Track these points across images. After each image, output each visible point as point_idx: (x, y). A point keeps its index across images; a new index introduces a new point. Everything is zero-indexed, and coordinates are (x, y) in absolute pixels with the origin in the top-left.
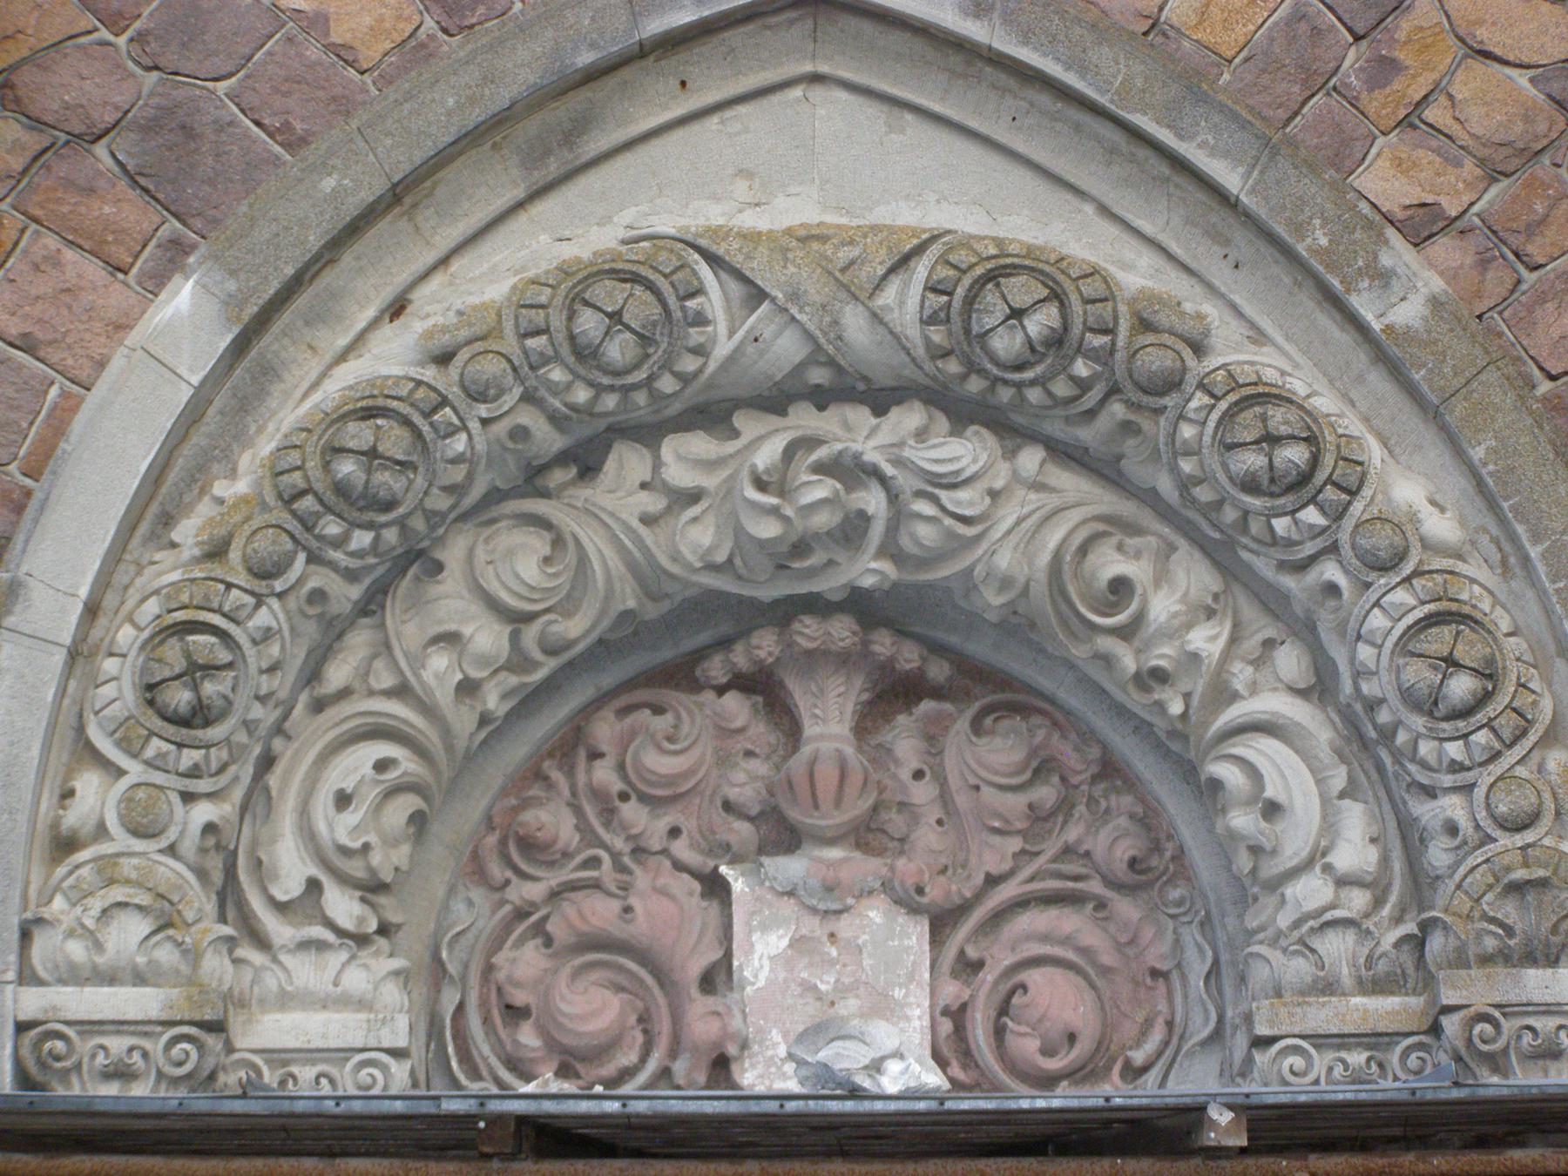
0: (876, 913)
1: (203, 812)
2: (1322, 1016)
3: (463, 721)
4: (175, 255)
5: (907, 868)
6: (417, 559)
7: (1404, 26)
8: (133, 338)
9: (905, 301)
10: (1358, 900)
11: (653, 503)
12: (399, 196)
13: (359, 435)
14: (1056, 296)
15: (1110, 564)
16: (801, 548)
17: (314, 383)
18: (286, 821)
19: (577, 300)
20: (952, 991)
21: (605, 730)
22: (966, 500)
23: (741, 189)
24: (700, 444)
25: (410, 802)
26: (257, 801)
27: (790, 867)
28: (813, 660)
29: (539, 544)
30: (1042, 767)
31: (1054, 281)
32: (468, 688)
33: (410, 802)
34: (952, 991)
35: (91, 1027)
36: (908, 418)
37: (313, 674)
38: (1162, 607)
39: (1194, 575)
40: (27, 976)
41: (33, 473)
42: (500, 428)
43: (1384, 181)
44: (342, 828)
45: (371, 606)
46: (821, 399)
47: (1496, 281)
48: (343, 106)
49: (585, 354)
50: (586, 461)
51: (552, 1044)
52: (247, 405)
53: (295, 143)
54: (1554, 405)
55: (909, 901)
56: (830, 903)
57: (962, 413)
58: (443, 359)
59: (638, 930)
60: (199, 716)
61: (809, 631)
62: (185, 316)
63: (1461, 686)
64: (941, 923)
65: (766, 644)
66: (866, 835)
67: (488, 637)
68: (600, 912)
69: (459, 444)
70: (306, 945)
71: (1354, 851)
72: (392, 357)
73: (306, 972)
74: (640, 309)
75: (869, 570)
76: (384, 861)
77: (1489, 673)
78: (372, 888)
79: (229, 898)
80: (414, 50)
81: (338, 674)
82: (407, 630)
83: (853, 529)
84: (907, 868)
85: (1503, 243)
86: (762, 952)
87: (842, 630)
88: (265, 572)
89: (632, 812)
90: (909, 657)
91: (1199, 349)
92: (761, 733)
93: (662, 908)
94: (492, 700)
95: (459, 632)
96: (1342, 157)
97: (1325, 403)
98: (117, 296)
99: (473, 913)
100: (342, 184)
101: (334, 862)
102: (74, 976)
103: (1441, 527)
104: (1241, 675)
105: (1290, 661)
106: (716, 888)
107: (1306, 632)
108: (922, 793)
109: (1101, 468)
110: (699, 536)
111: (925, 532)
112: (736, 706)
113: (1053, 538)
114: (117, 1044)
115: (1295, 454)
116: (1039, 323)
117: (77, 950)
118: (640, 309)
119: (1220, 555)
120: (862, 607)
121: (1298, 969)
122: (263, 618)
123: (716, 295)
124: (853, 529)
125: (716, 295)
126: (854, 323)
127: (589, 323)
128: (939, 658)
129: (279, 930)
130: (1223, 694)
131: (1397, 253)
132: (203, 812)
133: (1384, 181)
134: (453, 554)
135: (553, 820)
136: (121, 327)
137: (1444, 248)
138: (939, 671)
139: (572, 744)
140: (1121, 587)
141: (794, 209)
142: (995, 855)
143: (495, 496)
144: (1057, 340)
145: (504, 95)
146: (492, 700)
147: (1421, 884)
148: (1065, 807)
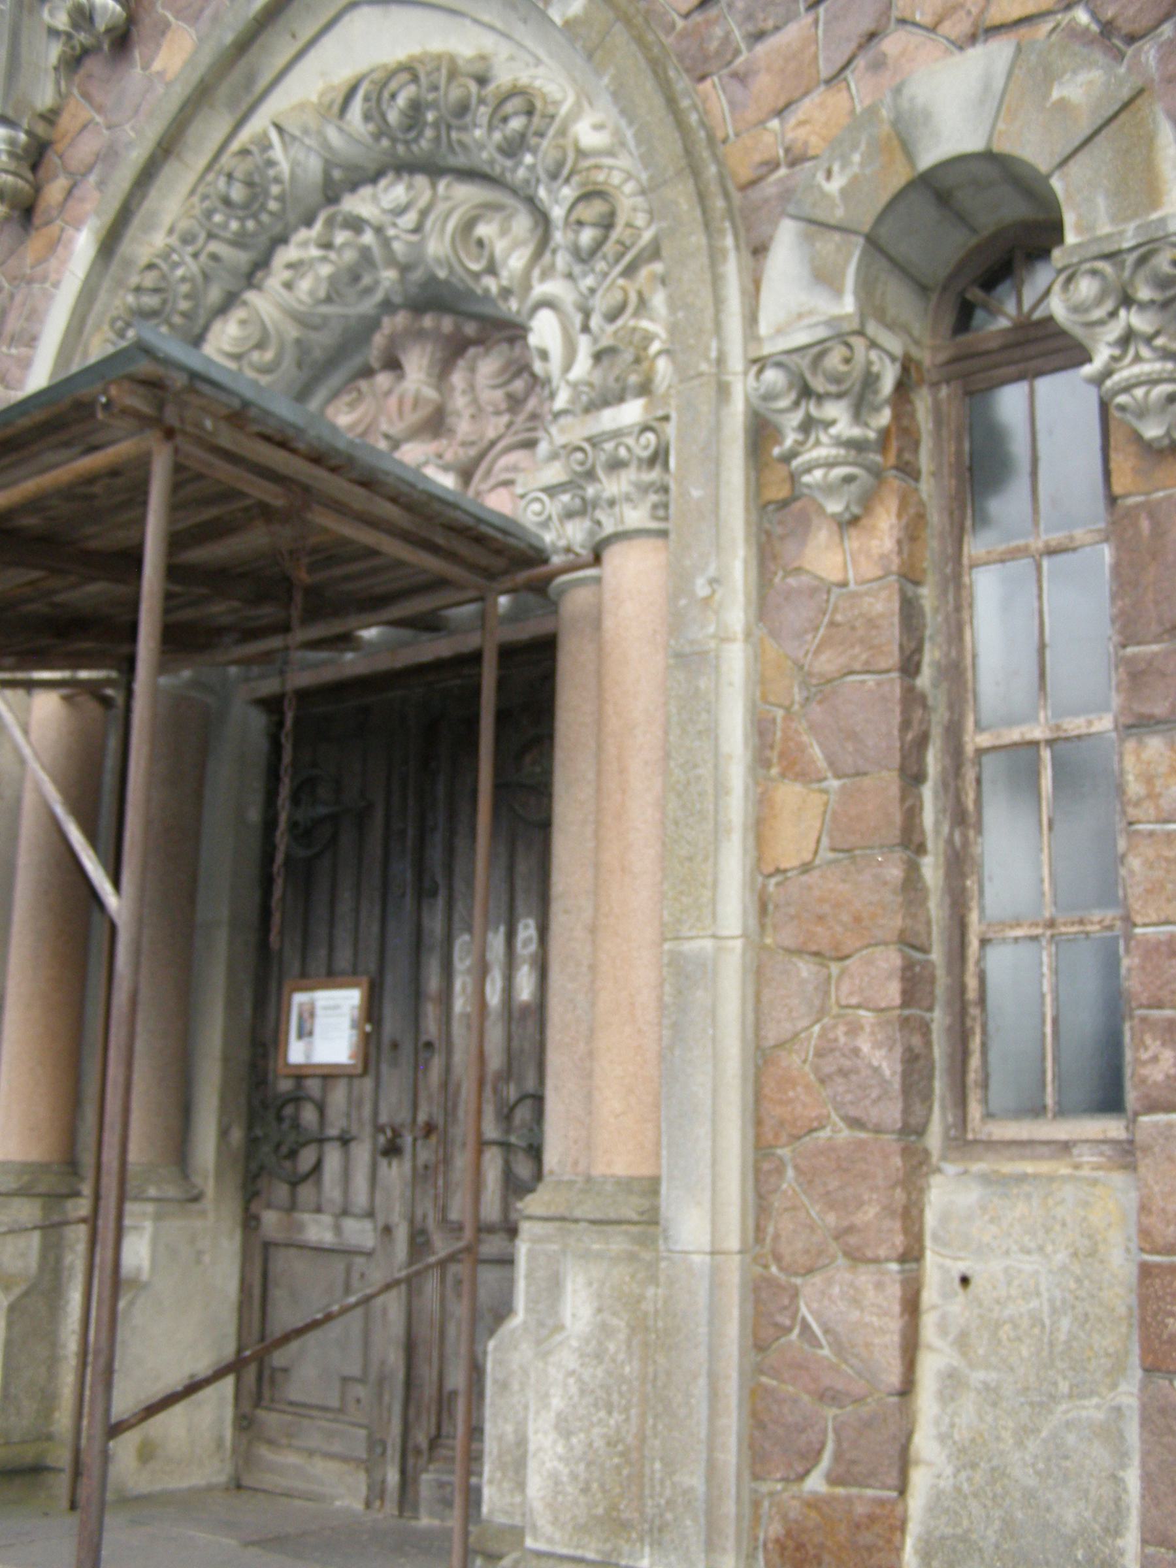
42: (203, 258)
69: (180, 272)
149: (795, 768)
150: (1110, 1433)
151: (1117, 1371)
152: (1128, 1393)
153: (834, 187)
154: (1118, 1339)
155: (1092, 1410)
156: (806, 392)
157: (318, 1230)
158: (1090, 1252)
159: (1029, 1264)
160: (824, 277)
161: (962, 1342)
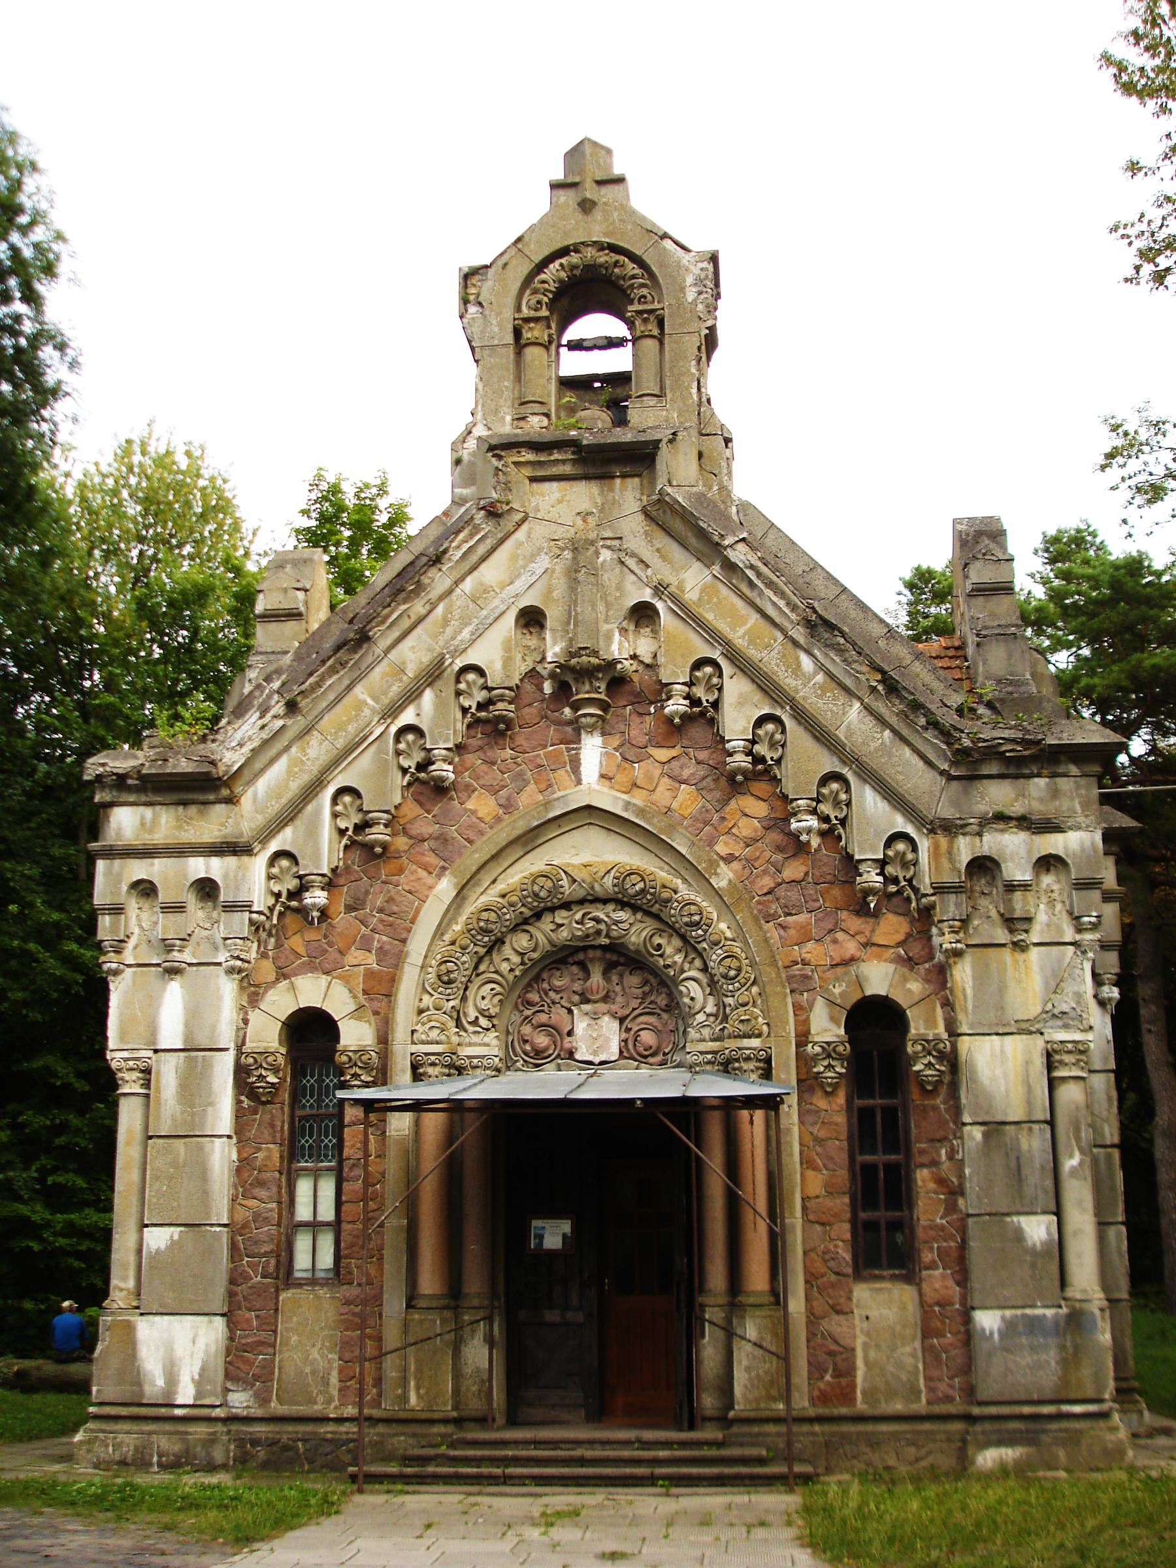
0: (606, 1018)
1: (452, 1003)
2: (702, 1047)
3: (511, 977)
4: (444, 869)
5: (614, 1008)
6: (500, 941)
7: (728, 809)
8: (435, 891)
9: (609, 881)
10: (712, 1019)
11: (552, 927)
12: (494, 857)
13: (485, 915)
14: (643, 879)
15: (657, 940)
16: (587, 936)
18: (470, 1002)
19: (534, 882)
20: (624, 1035)
21: (545, 975)
22: (625, 926)
23: (573, 851)
24: (564, 913)
25: (499, 997)
26: (464, 999)
27: (587, 1007)
28: (592, 960)
29: (527, 937)
30: (646, 982)
32: (512, 970)
33: (499, 997)
34: (624, 1035)
35: (426, 1054)
36: (610, 907)
37: (476, 967)
38: (669, 950)
39: (677, 942)
40: (413, 1043)
41: (412, 922)
44: (483, 1005)
45: (489, 952)
46: (591, 902)
47: (747, 871)
48: (481, 833)
49: (536, 895)
50: (538, 916)
51: (533, 1049)
52: (459, 907)
53: (471, 842)
54: (759, 903)
55: (613, 1015)
56: (595, 1017)
57: (622, 904)
58: (503, 896)
59: (553, 1021)
60: (450, 982)
61: (591, 953)
62: (445, 888)
63: (732, 973)
64: (622, 1020)
65: (581, 956)
66: (606, 999)
67: (516, 959)
68: (543, 1018)
70: (475, 1032)
71: (710, 1008)
72: (491, 897)
73: (475, 1039)
74: (549, 884)
75: (604, 941)
76: (493, 1012)
77: (739, 970)
78: (490, 1017)
79: (459, 1024)
80: (498, 819)
81: (482, 968)
82: (496, 956)
83: (599, 932)
84: (614, 1008)
85: (750, 862)
86: (581, 1026)
87: (598, 953)
88: (464, 948)
89: (551, 994)
90: (615, 958)
91: (676, 892)
92: (581, 975)
93: (558, 1015)
94: (517, 973)
95: (508, 960)
96: (711, 843)
97: (704, 904)
98: (430, 880)
99: (517, 1018)
100: (479, 857)
101: (482, 1012)
102: (423, 1043)
103: (729, 934)
104: (686, 966)
105: (698, 963)
106: (570, 1011)
107: (700, 955)
108: (618, 989)
109: (656, 917)
110: (564, 934)
111: (614, 934)
112: (575, 969)
113: (644, 934)
114: (433, 1058)
115: (697, 918)
116: (637, 888)
117: (424, 1037)
118: (549, 884)
119: (683, 937)
120: (601, 947)
121: (698, 1036)
122: (464, 959)
123: (565, 882)
124: (599, 932)
125: (565, 882)
126: (597, 887)
127: (536, 888)
128: (620, 958)
129: (471, 1029)
130: (683, 971)
131: (723, 868)
132: (452, 1003)
133: (721, 848)
134: (507, 940)
135: (534, 996)
136: (431, 888)
137: (736, 865)
138: (622, 960)
139: (537, 978)
140: (659, 946)
141: (586, 858)
142: (635, 1003)
143: (517, 925)
144: (643, 891)
145: (518, 832)
146: (517, 973)
147: (725, 1018)
148: (651, 991)
149: (815, 1169)
150: (913, 1355)
151: (914, 1338)
152: (917, 1344)
153: (837, 991)
155: (908, 1349)
156: (829, 1056)
157: (552, 1316)
158: (903, 1308)
159: (885, 1312)
160: (833, 1019)
161: (868, 1335)
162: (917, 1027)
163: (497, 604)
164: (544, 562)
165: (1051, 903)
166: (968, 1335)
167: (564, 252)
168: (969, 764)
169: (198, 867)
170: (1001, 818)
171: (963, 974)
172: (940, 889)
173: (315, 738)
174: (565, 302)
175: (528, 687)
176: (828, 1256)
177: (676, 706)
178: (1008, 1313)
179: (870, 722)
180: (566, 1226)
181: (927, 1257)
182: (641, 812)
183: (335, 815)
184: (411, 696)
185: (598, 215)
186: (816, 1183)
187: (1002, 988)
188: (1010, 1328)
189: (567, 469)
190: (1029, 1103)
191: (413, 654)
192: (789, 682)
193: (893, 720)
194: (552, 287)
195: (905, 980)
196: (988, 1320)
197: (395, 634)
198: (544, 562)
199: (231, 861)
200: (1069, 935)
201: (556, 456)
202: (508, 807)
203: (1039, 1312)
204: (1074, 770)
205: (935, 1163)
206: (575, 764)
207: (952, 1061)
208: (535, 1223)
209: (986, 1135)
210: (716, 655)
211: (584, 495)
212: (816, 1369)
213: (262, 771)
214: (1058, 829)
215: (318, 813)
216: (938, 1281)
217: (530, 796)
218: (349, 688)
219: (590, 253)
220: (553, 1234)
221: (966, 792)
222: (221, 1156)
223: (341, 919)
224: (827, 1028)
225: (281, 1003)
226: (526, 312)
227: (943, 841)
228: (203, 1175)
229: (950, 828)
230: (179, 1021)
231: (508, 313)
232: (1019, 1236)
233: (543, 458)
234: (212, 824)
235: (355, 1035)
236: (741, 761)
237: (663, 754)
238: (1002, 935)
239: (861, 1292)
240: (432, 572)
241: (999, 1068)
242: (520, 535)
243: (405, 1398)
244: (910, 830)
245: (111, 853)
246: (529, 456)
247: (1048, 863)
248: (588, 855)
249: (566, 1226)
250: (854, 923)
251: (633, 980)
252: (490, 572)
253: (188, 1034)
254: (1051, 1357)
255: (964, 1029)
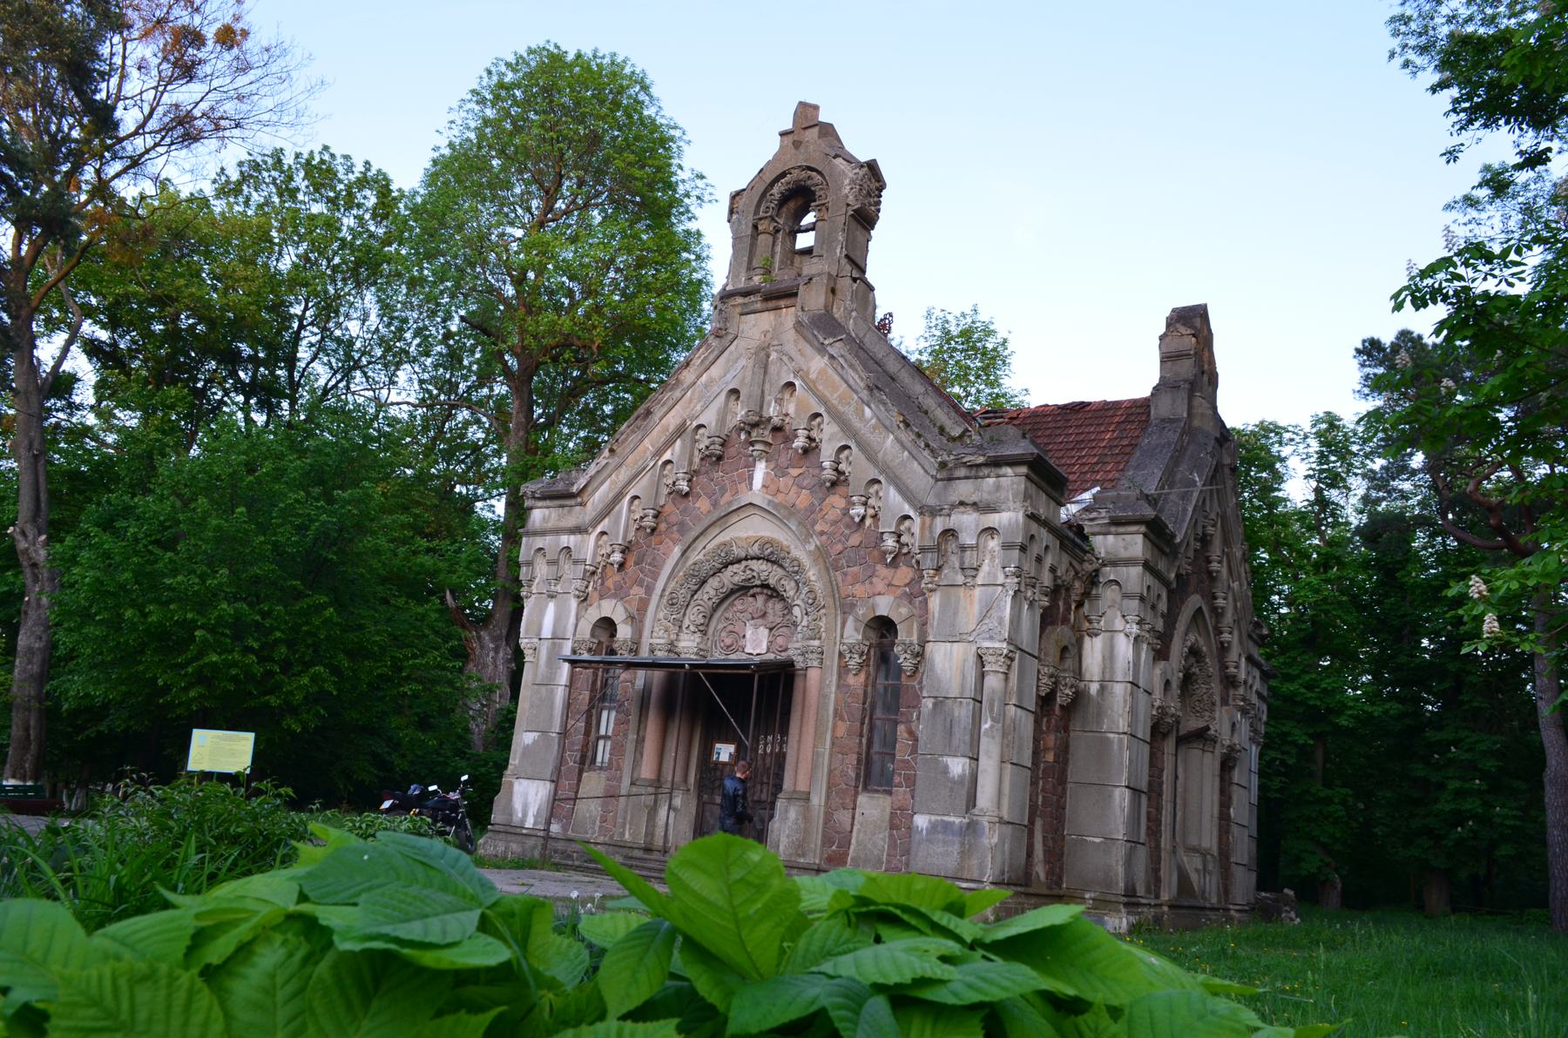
6: (704, 582)
9: (756, 547)
17: (696, 556)
31: (770, 542)
43: (818, 528)
56: (756, 627)
62: (677, 551)
86: (749, 634)
110: (736, 579)
133: (818, 528)
149: (842, 719)
154: (886, 824)
160: (857, 630)
162: (902, 636)
163: (716, 389)
164: (742, 362)
165: (993, 557)
166: (910, 828)
167: (783, 175)
168: (946, 473)
169: (565, 540)
170: (962, 503)
171: (935, 602)
172: (923, 550)
173: (623, 470)
174: (792, 205)
175: (734, 435)
176: (844, 774)
177: (800, 443)
178: (933, 818)
179: (897, 447)
180: (731, 748)
181: (897, 779)
182: (776, 506)
183: (630, 511)
184: (669, 443)
185: (802, 149)
186: (842, 729)
187: (956, 614)
188: (933, 827)
189: (759, 306)
190: (963, 686)
191: (672, 420)
192: (857, 424)
193: (909, 445)
194: (777, 196)
195: (898, 606)
196: (921, 821)
197: (665, 409)
198: (742, 362)
199: (579, 537)
200: (1001, 579)
201: (752, 298)
202: (715, 505)
203: (952, 819)
204: (1009, 470)
205: (909, 722)
206: (751, 478)
207: (920, 655)
208: (718, 746)
209: (935, 705)
210: (822, 410)
211: (765, 320)
212: (827, 841)
213: (597, 488)
214: (995, 511)
215: (620, 511)
216: (901, 792)
217: (727, 497)
218: (641, 441)
219: (796, 175)
220: (724, 752)
221: (945, 488)
222: (560, 694)
223: (631, 568)
224: (853, 634)
225: (593, 615)
226: (761, 214)
227: (928, 520)
228: (553, 703)
229: (934, 512)
230: (552, 622)
231: (751, 217)
232: (946, 770)
233: (746, 300)
234: (575, 516)
235: (624, 632)
236: (829, 474)
237: (794, 472)
238: (960, 579)
239: (863, 799)
240: (685, 373)
241: (949, 663)
242: (732, 347)
243: (623, 834)
244: (912, 513)
245: (528, 534)
246: (740, 300)
247: (991, 531)
248: (748, 531)
249: (731, 748)
250: (882, 571)
251: (779, 606)
252: (715, 371)
253: (554, 632)
254: (955, 849)
255: (931, 638)
